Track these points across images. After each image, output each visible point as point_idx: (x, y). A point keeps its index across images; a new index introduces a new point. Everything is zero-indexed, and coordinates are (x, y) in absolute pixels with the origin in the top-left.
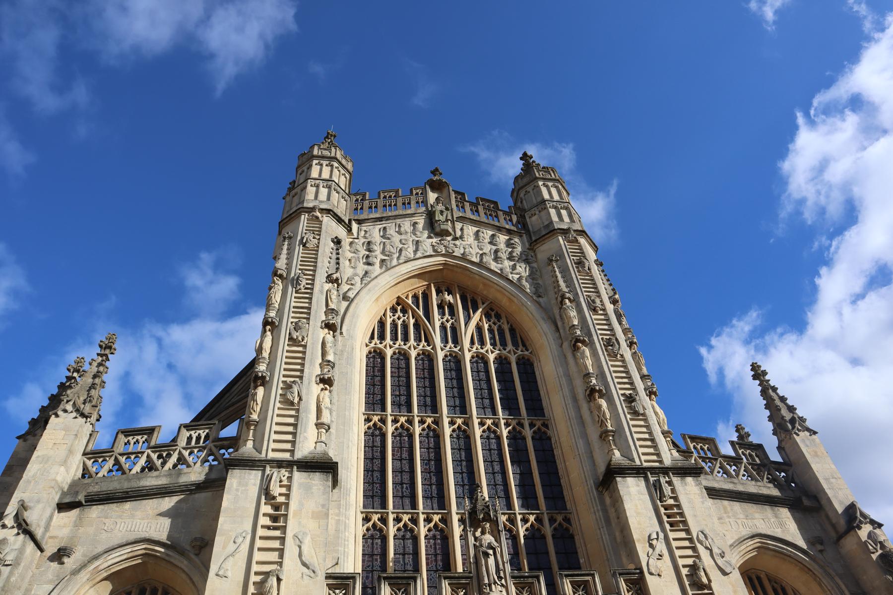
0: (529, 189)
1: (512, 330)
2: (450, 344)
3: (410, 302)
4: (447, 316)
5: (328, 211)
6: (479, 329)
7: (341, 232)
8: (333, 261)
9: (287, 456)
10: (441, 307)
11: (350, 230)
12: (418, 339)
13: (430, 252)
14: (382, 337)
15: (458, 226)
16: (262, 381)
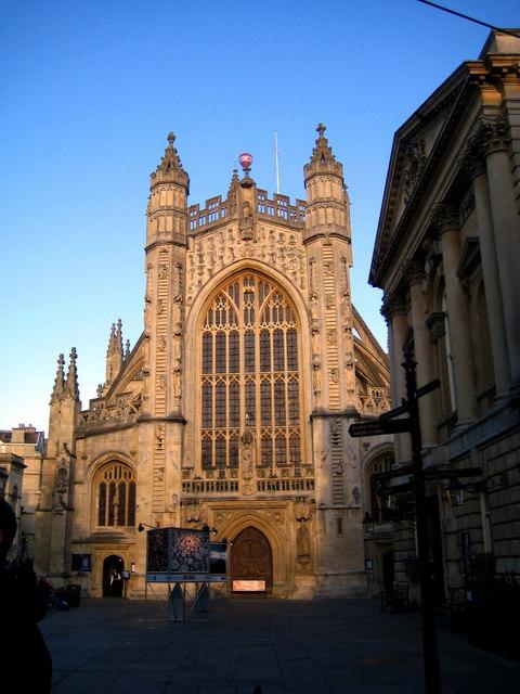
0: (311, 182)
1: (288, 307)
2: (249, 324)
3: (226, 294)
4: (249, 302)
5: (171, 243)
6: (267, 309)
7: (182, 250)
8: (177, 284)
9: (162, 416)
10: (246, 293)
11: (188, 249)
12: (231, 322)
13: (238, 257)
14: (211, 323)
15: (258, 227)
16: (147, 373)
